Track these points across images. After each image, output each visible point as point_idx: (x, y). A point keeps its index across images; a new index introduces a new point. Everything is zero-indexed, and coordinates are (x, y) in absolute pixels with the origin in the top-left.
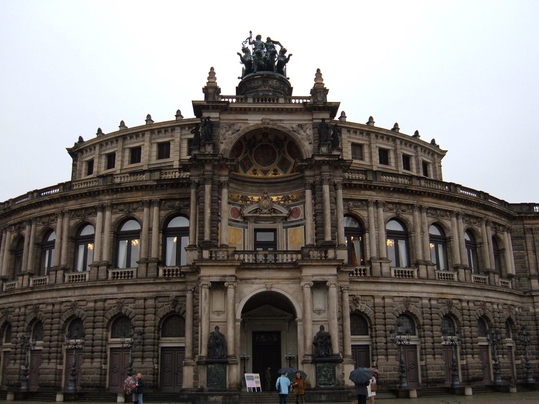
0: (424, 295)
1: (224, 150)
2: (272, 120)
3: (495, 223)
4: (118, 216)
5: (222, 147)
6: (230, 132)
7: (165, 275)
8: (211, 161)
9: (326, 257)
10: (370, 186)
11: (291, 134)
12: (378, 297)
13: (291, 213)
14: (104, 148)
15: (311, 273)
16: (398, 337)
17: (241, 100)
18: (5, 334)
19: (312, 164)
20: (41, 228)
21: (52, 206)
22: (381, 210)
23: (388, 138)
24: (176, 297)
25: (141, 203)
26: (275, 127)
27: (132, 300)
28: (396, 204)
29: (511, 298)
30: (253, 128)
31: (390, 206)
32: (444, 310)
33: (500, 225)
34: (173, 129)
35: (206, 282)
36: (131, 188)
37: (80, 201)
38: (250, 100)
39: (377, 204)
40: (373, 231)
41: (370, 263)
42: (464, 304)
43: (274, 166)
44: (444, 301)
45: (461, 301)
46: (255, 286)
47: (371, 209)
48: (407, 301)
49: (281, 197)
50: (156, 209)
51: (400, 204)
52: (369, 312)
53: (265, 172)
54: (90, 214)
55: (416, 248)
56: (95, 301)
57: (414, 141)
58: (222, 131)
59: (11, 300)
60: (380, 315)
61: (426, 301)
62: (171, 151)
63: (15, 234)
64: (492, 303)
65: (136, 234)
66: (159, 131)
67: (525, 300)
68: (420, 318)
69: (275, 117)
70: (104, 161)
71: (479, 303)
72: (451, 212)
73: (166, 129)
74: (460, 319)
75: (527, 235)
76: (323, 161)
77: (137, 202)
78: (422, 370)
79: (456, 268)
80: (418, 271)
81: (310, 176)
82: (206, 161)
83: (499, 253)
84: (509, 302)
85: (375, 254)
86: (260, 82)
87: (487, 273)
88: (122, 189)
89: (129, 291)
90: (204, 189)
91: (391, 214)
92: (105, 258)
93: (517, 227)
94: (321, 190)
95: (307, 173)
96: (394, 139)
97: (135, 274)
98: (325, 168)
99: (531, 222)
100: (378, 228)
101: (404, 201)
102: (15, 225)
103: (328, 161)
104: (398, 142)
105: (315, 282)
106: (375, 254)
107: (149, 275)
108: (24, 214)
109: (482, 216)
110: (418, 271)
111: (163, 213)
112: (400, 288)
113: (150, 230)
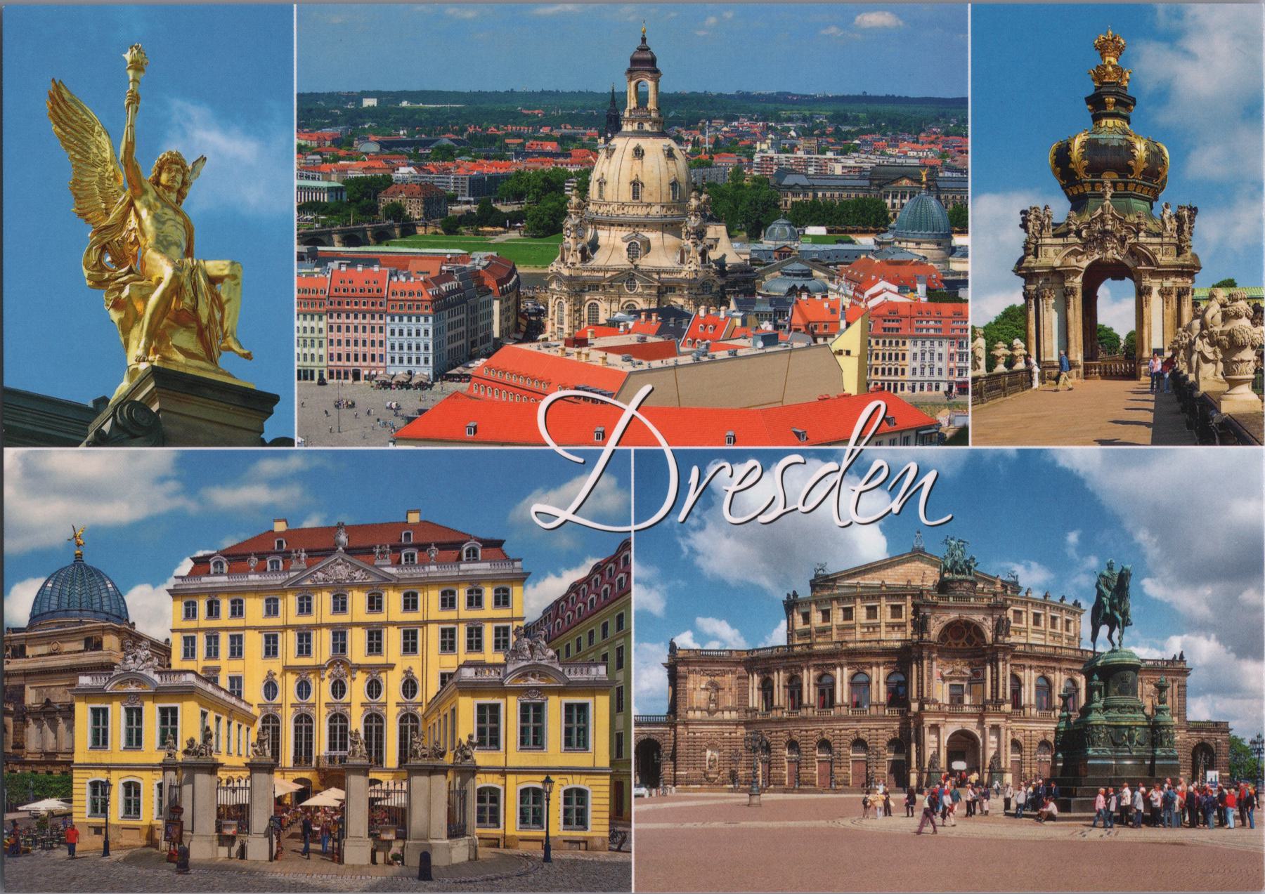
39: (1031, 668)
40: (1027, 687)
41: (1023, 708)
52: (1021, 740)
70: (820, 615)
92: (846, 700)
111: (887, 671)
113: (878, 682)
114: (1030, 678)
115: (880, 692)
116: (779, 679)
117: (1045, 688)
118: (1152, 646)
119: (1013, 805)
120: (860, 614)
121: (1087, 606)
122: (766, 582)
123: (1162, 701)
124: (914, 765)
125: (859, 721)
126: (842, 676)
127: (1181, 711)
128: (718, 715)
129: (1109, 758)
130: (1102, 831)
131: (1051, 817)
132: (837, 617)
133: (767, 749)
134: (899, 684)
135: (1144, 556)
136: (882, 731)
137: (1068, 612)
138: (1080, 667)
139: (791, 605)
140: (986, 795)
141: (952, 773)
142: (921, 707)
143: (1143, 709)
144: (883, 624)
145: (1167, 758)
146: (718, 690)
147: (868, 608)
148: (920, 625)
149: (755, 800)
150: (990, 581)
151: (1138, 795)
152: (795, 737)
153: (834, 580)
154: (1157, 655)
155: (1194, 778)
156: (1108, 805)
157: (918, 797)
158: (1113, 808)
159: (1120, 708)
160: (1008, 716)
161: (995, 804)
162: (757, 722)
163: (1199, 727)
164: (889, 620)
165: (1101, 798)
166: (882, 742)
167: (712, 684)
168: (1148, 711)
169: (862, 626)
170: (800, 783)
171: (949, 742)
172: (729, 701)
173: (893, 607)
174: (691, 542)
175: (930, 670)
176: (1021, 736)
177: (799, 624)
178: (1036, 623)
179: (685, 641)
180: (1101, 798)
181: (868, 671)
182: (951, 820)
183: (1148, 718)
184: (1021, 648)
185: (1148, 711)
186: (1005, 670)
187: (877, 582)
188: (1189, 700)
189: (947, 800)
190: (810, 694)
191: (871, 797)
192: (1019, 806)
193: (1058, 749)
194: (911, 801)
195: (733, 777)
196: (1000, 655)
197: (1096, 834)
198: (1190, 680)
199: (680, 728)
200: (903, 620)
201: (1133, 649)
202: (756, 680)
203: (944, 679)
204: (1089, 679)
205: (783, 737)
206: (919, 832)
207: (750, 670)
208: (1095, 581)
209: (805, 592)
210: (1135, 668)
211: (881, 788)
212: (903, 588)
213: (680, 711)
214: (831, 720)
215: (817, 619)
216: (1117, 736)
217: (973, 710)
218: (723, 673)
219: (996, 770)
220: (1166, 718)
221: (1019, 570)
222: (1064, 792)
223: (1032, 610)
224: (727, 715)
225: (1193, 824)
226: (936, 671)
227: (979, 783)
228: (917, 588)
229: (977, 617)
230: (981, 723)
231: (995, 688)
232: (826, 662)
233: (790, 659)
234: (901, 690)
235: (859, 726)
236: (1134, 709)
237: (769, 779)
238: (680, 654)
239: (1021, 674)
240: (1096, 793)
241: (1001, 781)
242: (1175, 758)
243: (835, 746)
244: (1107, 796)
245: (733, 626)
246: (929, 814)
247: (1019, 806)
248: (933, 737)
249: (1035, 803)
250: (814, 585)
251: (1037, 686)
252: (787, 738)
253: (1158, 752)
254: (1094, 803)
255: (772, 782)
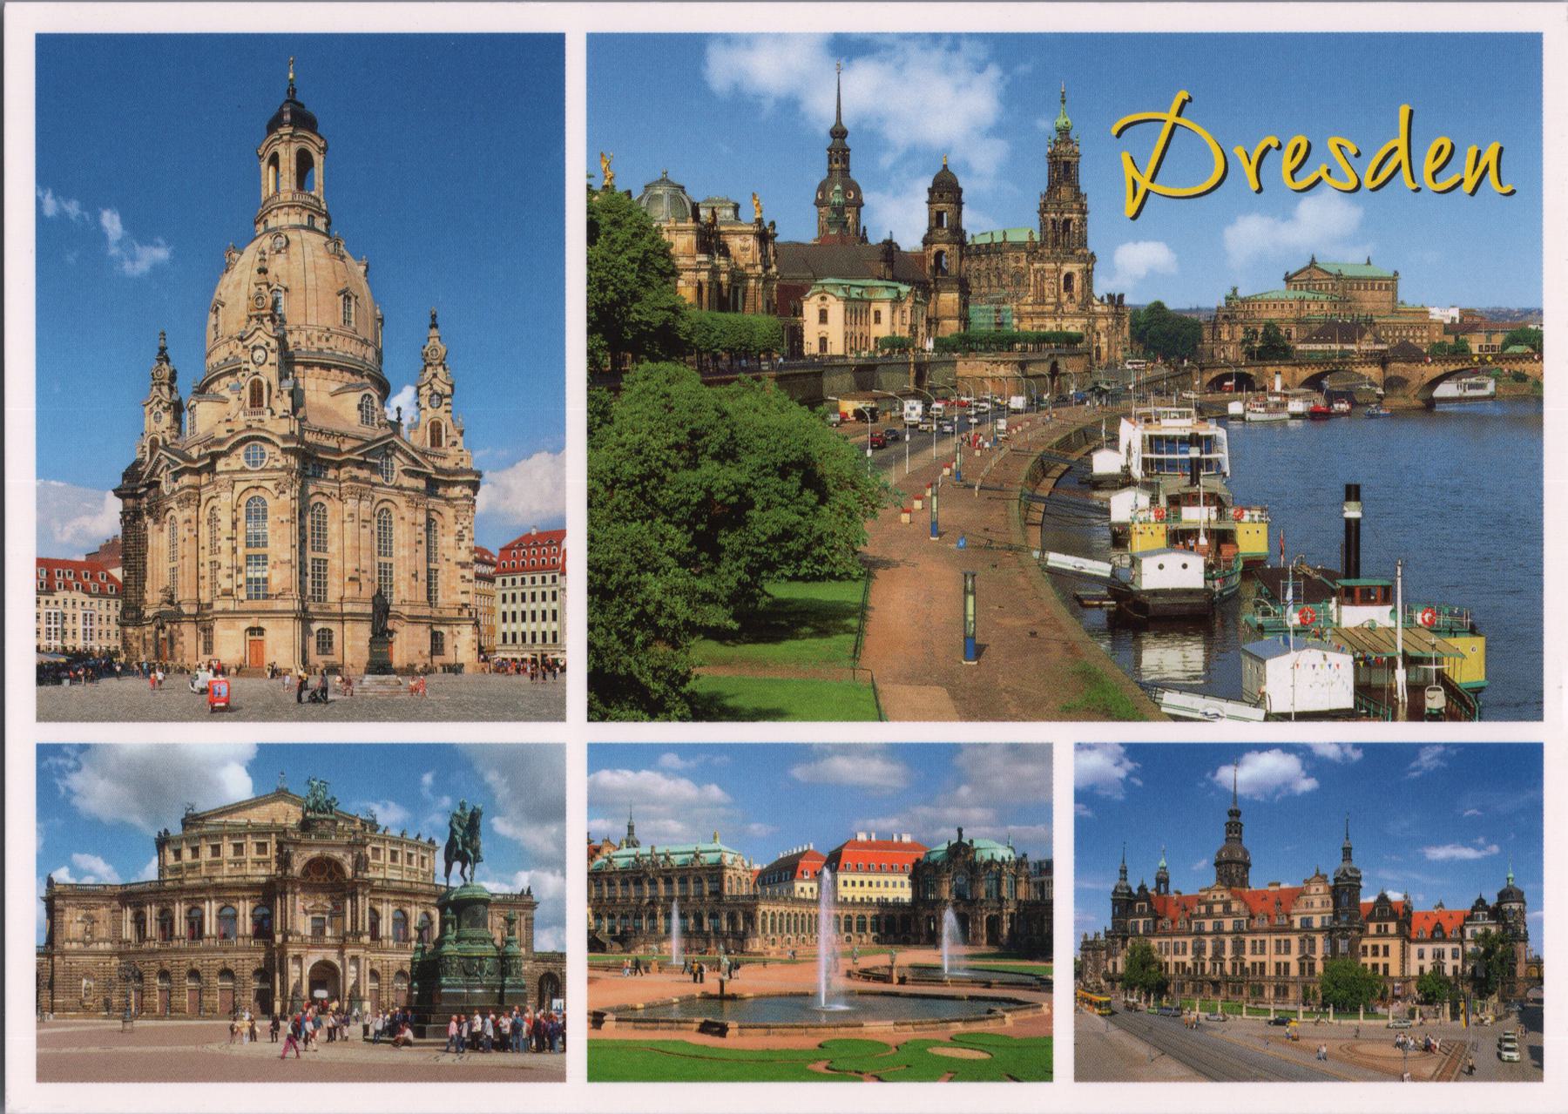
114: (387, 911)
115: (246, 925)
116: (151, 912)
117: (402, 920)
118: (501, 881)
119: (371, 1031)
120: (228, 850)
121: (441, 844)
122: (137, 820)
123: (511, 933)
124: (278, 993)
126: (210, 909)
127: (529, 944)
128: (94, 947)
129: (460, 987)
130: (454, 1056)
131: (407, 1043)
132: (206, 854)
133: (140, 978)
134: (264, 917)
135: (494, 796)
136: (248, 960)
137: (423, 849)
138: (434, 901)
139: (162, 842)
140: (346, 1022)
141: (314, 1001)
142: (285, 939)
143: (492, 941)
145: (515, 986)
147: (235, 845)
148: (284, 861)
149: (128, 1026)
150: (351, 820)
151: (488, 1021)
152: (167, 967)
153: (203, 819)
154: (506, 890)
155: (540, 1006)
156: (460, 1032)
157: (282, 1023)
158: (465, 1034)
159: (471, 940)
160: (366, 947)
161: (354, 1030)
162: (129, 953)
163: (544, 958)
164: (255, 856)
165: (453, 1025)
166: (248, 972)
167: (88, 917)
168: (498, 943)
169: (230, 862)
170: (170, 1010)
172: (103, 931)
173: (258, 844)
174: (68, 783)
175: (294, 904)
176: (378, 966)
177: (170, 859)
178: (394, 859)
179: (62, 876)
180: (453, 1025)
182: (313, 1045)
183: (498, 949)
184: (378, 883)
185: (498, 943)
186: (364, 904)
187: (243, 821)
188: (536, 933)
189: (309, 1026)
190: (181, 927)
191: (238, 1024)
192: (377, 1032)
193: (414, 978)
194: (276, 1027)
195: (107, 1005)
196: (360, 890)
197: (449, 1059)
198: (537, 913)
199: (57, 959)
201: (485, 884)
202: (128, 914)
203: (306, 912)
204: (443, 912)
205: (156, 967)
206: (283, 1057)
207: (124, 904)
208: (448, 820)
209: (176, 830)
210: (486, 902)
211: (247, 1016)
212: (267, 826)
213: (58, 939)
214: (199, 951)
215: (187, 855)
216: (469, 967)
217: (333, 941)
218: (98, 906)
219: (355, 998)
220: (514, 949)
221: (377, 809)
222: (418, 1020)
223: (389, 847)
224: (101, 946)
225: (539, 1050)
226: (299, 904)
227: (339, 1011)
228: (281, 826)
229: (338, 854)
230: (341, 954)
231: (355, 921)
232: (195, 896)
233: (160, 893)
234: (266, 923)
235: (226, 957)
236: (484, 941)
237: (141, 1007)
238: (57, 889)
239: (378, 907)
240: (450, 1020)
241: (360, 1009)
242: (523, 987)
243: (204, 974)
244: (459, 1023)
245: (107, 861)
246: (292, 1039)
247: (377, 1032)
248: (296, 967)
249: (392, 1029)
250: (185, 823)
251: (395, 920)
253: (507, 981)
254: (447, 1029)
255: (144, 1010)
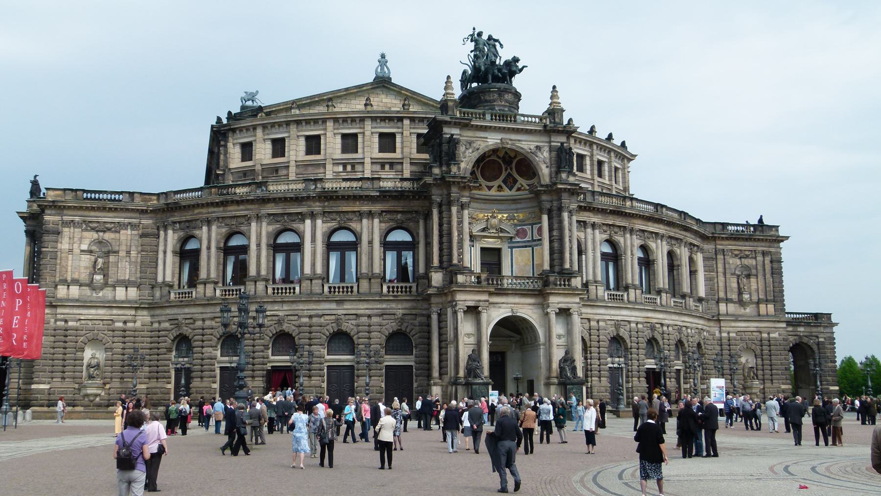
0: (632, 319)
1: (466, 169)
2: (511, 140)
3: (691, 244)
4: (329, 225)
5: (463, 165)
6: (470, 151)
7: (389, 292)
8: (459, 183)
9: (569, 285)
10: (590, 208)
11: (529, 156)
12: (594, 320)
13: (518, 233)
14: (267, 132)
15: (556, 301)
16: (617, 359)
17: (480, 114)
18: (174, 348)
19: (552, 189)
20: (224, 230)
21: (242, 207)
22: (597, 231)
23: (586, 142)
24: (404, 315)
25: (358, 214)
26: (514, 147)
27: (354, 317)
28: (610, 225)
29: (701, 322)
30: (492, 147)
31: (605, 228)
32: (648, 333)
33: (694, 245)
34: (362, 119)
35: (461, 307)
36: (349, 197)
37: (281, 205)
38: (488, 117)
42: (665, 328)
43: (499, 182)
44: (649, 325)
45: (662, 325)
46: (502, 310)
47: (589, 230)
48: (617, 325)
49: (505, 215)
50: (376, 221)
51: (613, 225)
53: (490, 188)
54: (294, 221)
55: (626, 271)
56: (310, 317)
57: (607, 145)
58: (462, 149)
59: (187, 310)
60: (594, 337)
61: (633, 325)
62: (360, 145)
63: (182, 234)
64: (687, 327)
65: (353, 246)
66: (345, 120)
67: (712, 324)
68: (628, 341)
69: (514, 137)
70: (269, 146)
71: (676, 327)
72: (657, 234)
73: (353, 120)
74: (661, 343)
75: (718, 257)
76: (565, 189)
77: (354, 212)
78: (628, 392)
79: (659, 292)
80: (628, 294)
81: (547, 201)
82: (454, 182)
83: (693, 273)
84: (700, 327)
85: (591, 278)
86: (496, 96)
87: (683, 296)
88: (337, 197)
89: (349, 307)
90: (450, 211)
91: (605, 236)
92: (319, 270)
93: (709, 247)
94: (560, 215)
95: (544, 197)
96: (591, 144)
97: (355, 289)
98: (565, 195)
99: (724, 243)
100: (594, 250)
101: (618, 223)
102: (180, 222)
103: (569, 189)
104: (595, 147)
105: (560, 309)
106: (591, 278)
107: (372, 291)
108: (196, 211)
109: (682, 237)
110: (628, 294)
112: (613, 312)
113: (371, 242)
125: (340, 302)
144: (368, 161)
146: (108, 254)
166: (378, 339)
171: (494, 335)
181: (354, 225)
200: (398, 155)
202: (171, 238)
218: (118, 227)
251: (604, 256)
252: (221, 330)
